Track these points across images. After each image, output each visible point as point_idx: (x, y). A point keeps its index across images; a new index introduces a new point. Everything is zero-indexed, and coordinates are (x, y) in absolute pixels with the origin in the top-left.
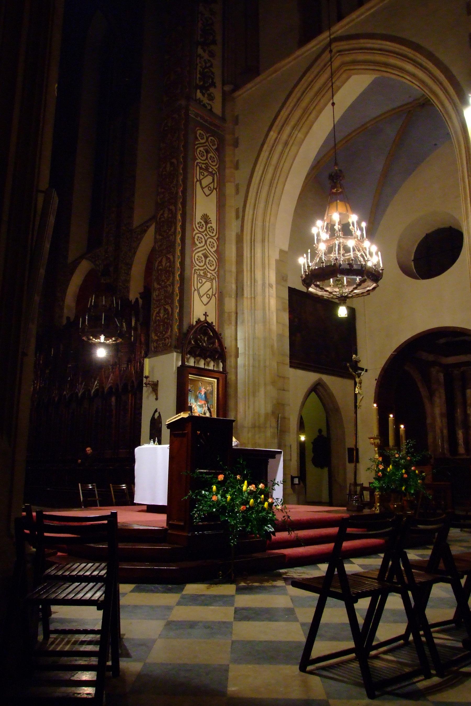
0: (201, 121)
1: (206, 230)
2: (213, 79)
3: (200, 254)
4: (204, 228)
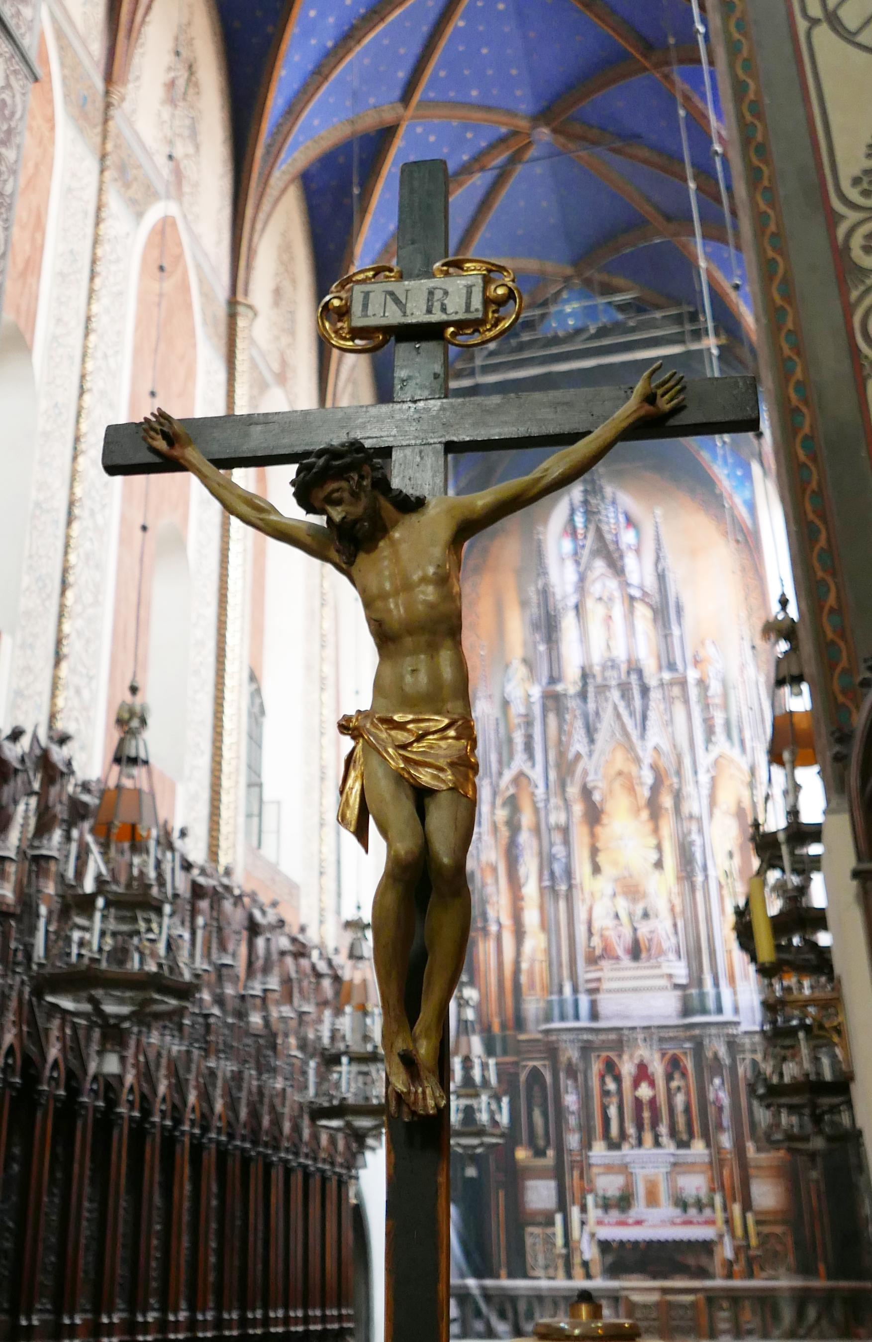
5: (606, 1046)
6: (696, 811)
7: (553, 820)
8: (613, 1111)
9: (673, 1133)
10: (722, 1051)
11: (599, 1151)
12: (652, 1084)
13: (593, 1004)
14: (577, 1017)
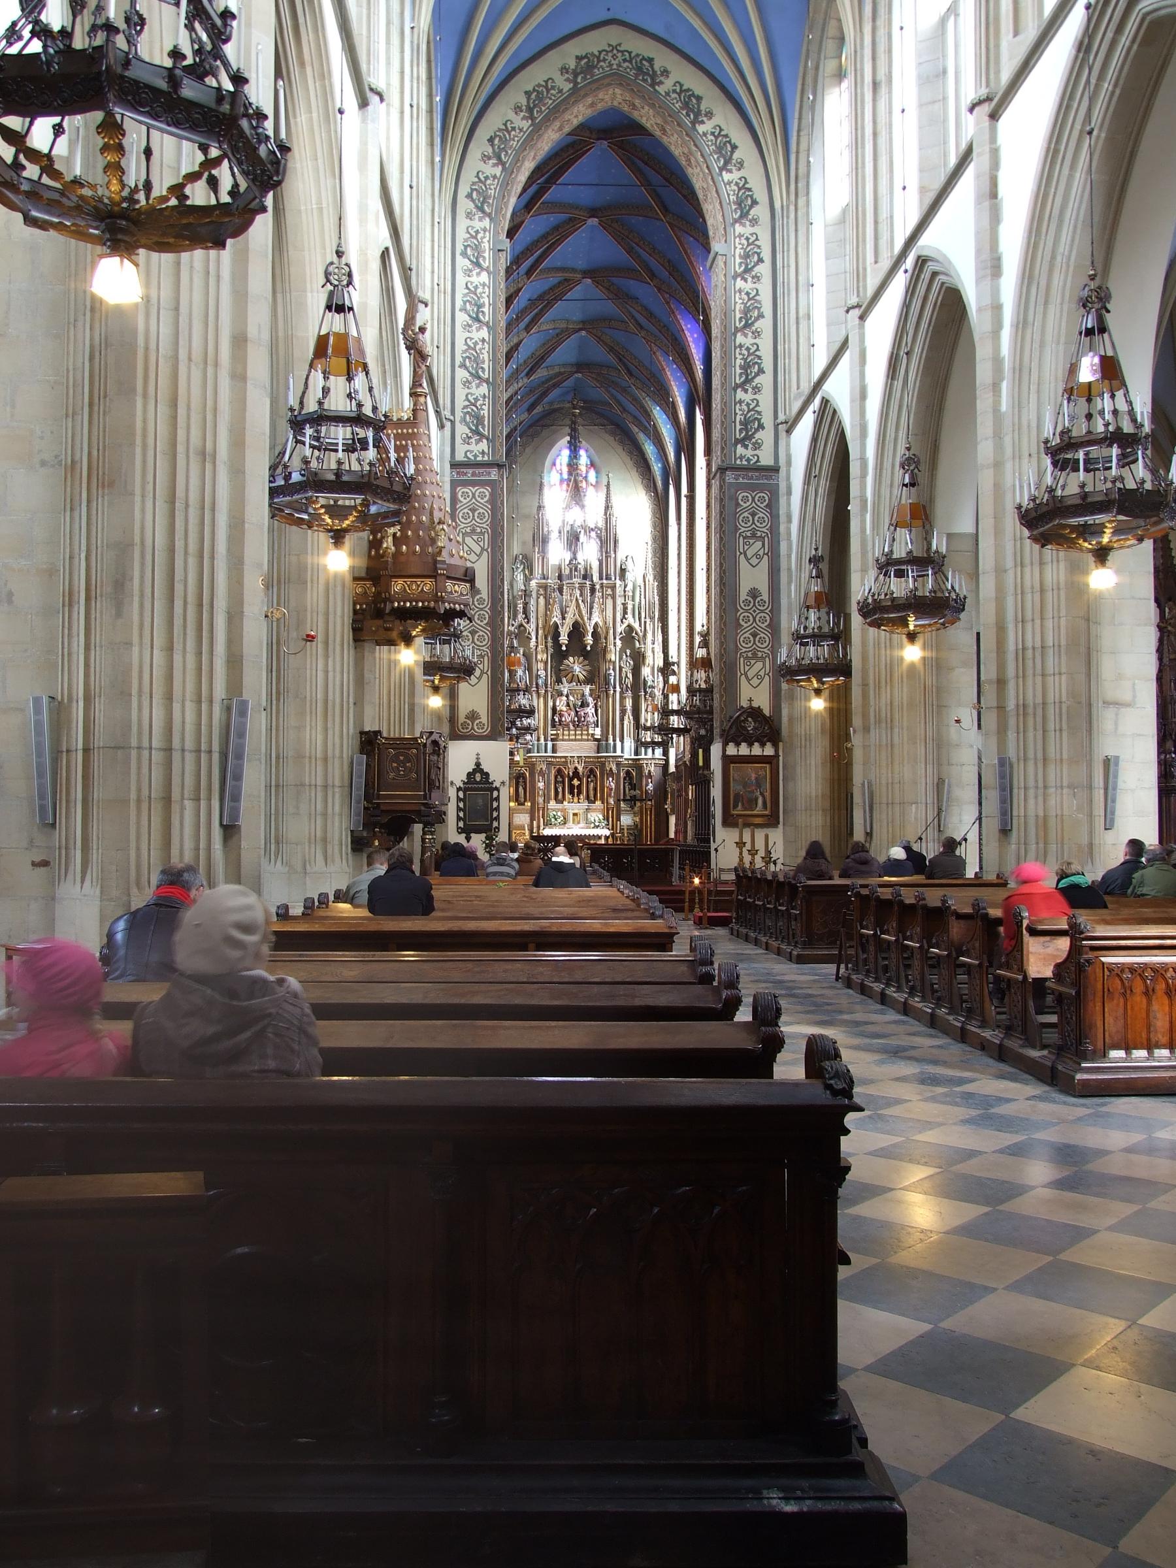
0: (746, 481)
1: (754, 605)
2: (759, 420)
3: (747, 635)
4: (752, 604)
5: (558, 763)
6: (613, 659)
7: (539, 657)
8: (560, 790)
9: (588, 798)
10: (614, 768)
11: (552, 804)
12: (579, 779)
13: (554, 746)
14: (546, 752)
